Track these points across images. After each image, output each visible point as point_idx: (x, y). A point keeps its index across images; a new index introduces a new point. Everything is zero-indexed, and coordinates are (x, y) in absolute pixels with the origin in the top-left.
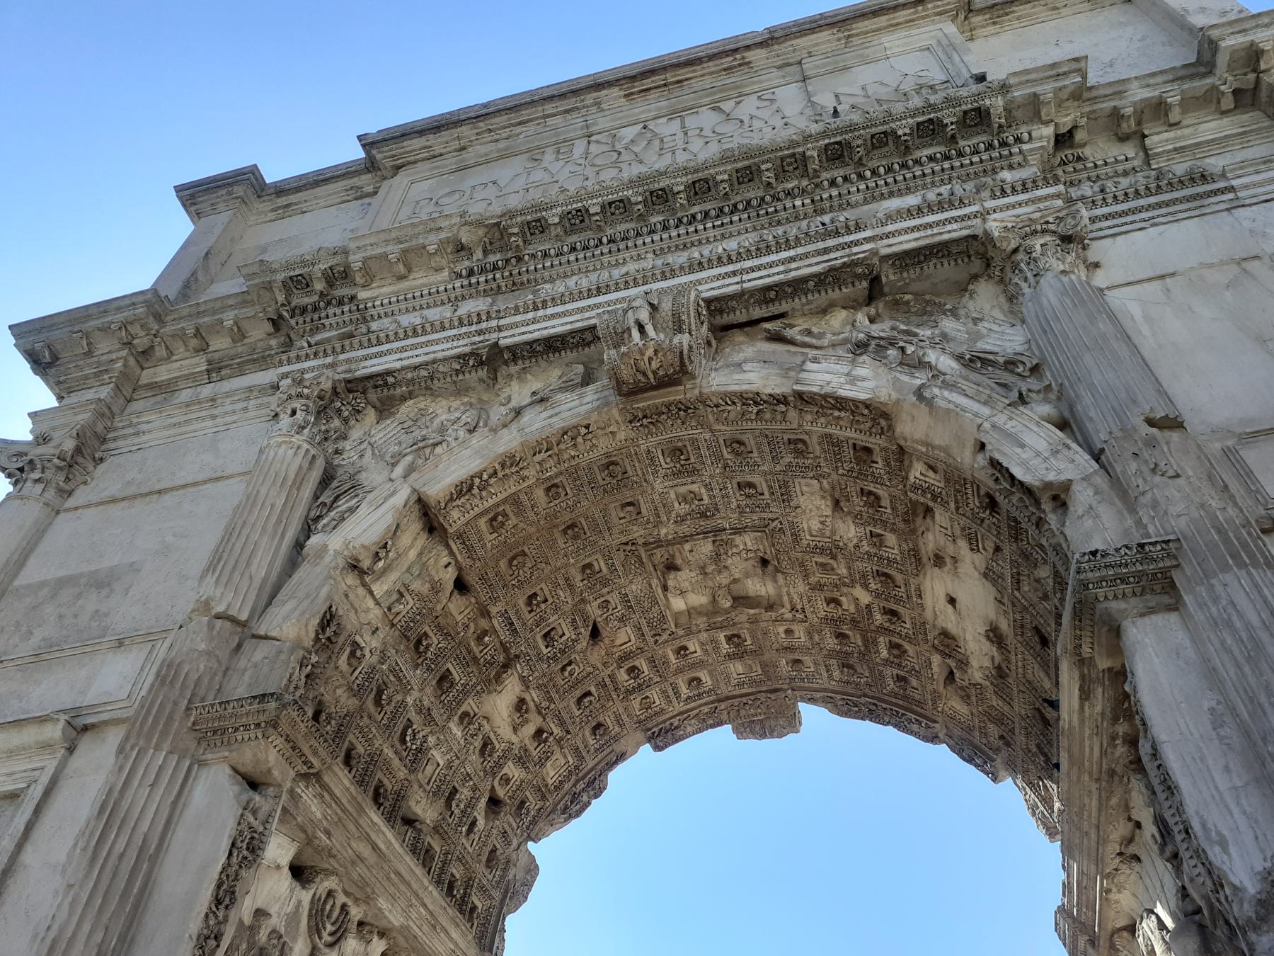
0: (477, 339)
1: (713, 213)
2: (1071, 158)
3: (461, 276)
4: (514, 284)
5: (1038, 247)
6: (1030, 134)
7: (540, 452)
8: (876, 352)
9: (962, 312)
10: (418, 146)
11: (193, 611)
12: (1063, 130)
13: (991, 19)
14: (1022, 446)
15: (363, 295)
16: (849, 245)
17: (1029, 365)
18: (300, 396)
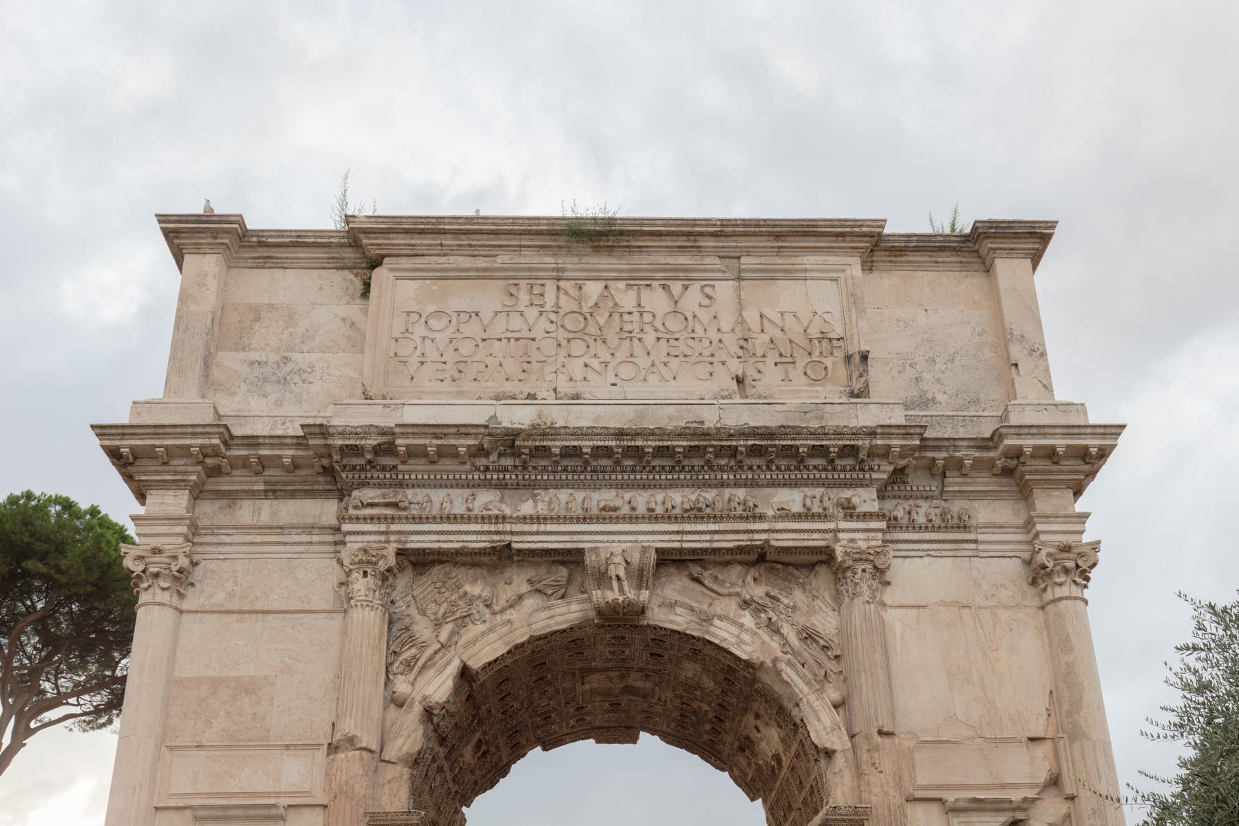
0: (496, 538)
1: (667, 469)
2: (899, 480)
3: (479, 470)
4: (518, 484)
5: (860, 570)
6: (879, 466)
7: (539, 640)
8: (754, 611)
9: (808, 587)
10: (402, 242)
11: (341, 740)
12: (899, 467)
13: (889, 256)
14: (819, 720)
15: (400, 467)
16: (753, 532)
17: (835, 654)
18: (369, 562)
